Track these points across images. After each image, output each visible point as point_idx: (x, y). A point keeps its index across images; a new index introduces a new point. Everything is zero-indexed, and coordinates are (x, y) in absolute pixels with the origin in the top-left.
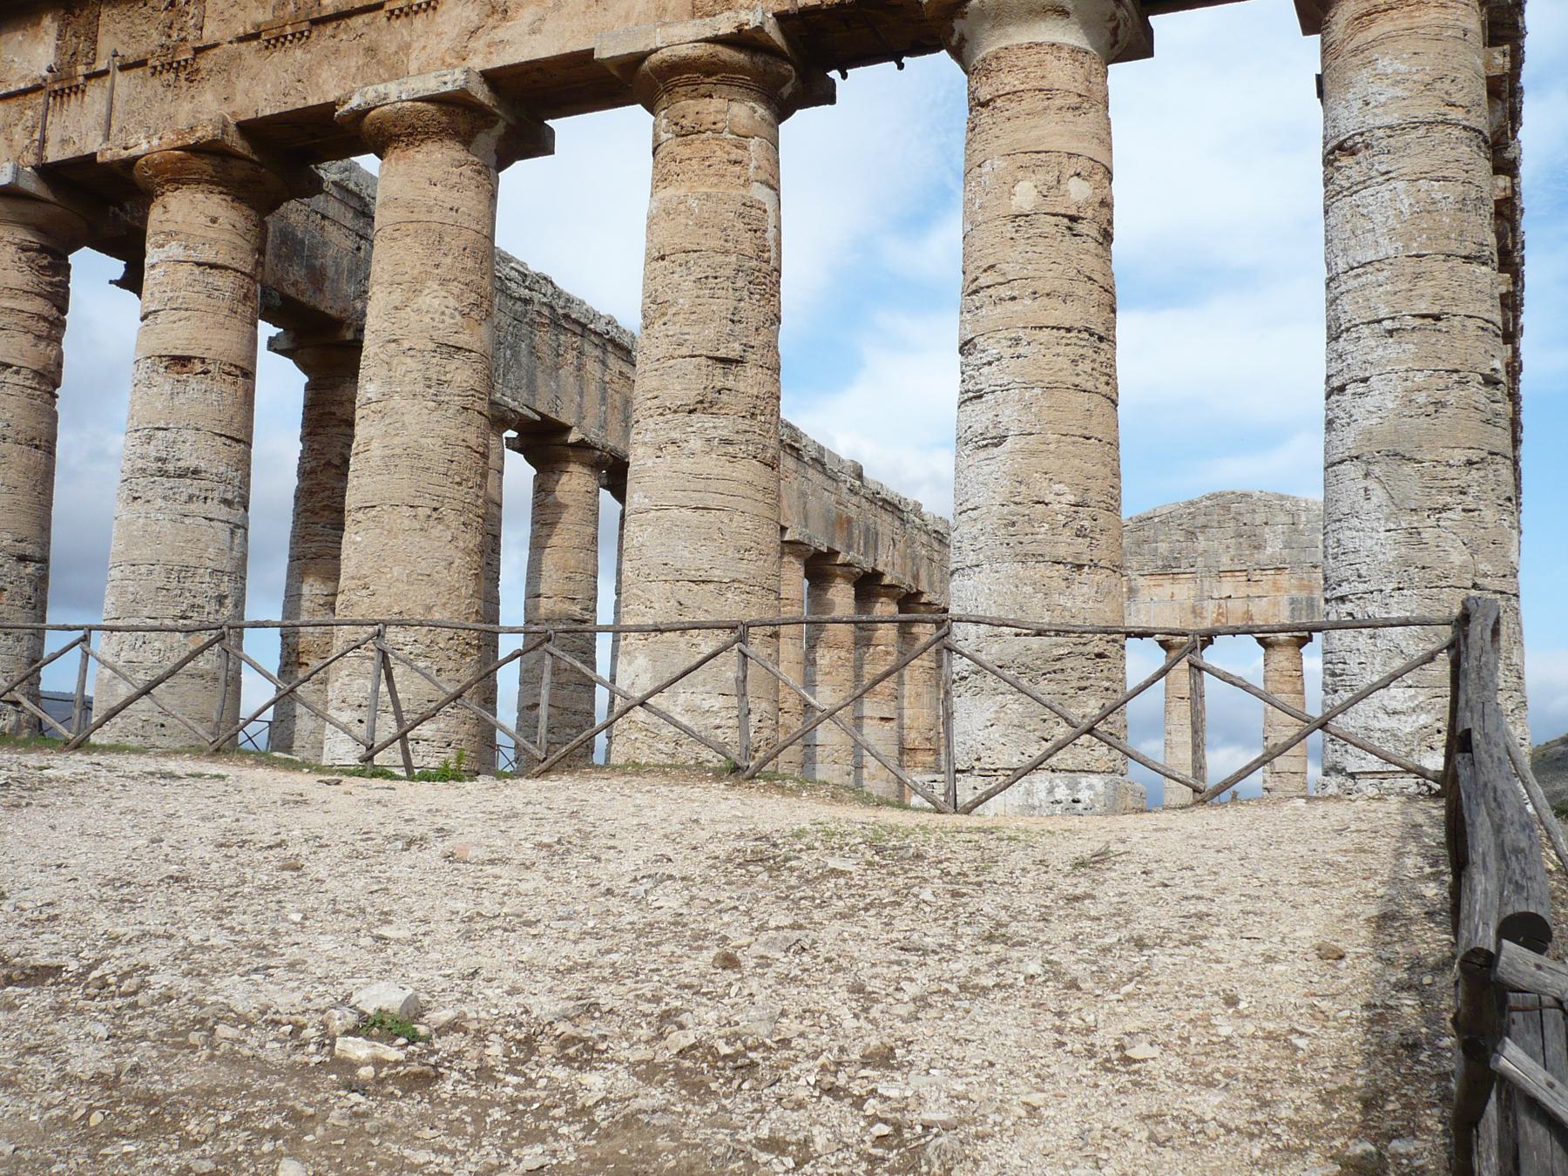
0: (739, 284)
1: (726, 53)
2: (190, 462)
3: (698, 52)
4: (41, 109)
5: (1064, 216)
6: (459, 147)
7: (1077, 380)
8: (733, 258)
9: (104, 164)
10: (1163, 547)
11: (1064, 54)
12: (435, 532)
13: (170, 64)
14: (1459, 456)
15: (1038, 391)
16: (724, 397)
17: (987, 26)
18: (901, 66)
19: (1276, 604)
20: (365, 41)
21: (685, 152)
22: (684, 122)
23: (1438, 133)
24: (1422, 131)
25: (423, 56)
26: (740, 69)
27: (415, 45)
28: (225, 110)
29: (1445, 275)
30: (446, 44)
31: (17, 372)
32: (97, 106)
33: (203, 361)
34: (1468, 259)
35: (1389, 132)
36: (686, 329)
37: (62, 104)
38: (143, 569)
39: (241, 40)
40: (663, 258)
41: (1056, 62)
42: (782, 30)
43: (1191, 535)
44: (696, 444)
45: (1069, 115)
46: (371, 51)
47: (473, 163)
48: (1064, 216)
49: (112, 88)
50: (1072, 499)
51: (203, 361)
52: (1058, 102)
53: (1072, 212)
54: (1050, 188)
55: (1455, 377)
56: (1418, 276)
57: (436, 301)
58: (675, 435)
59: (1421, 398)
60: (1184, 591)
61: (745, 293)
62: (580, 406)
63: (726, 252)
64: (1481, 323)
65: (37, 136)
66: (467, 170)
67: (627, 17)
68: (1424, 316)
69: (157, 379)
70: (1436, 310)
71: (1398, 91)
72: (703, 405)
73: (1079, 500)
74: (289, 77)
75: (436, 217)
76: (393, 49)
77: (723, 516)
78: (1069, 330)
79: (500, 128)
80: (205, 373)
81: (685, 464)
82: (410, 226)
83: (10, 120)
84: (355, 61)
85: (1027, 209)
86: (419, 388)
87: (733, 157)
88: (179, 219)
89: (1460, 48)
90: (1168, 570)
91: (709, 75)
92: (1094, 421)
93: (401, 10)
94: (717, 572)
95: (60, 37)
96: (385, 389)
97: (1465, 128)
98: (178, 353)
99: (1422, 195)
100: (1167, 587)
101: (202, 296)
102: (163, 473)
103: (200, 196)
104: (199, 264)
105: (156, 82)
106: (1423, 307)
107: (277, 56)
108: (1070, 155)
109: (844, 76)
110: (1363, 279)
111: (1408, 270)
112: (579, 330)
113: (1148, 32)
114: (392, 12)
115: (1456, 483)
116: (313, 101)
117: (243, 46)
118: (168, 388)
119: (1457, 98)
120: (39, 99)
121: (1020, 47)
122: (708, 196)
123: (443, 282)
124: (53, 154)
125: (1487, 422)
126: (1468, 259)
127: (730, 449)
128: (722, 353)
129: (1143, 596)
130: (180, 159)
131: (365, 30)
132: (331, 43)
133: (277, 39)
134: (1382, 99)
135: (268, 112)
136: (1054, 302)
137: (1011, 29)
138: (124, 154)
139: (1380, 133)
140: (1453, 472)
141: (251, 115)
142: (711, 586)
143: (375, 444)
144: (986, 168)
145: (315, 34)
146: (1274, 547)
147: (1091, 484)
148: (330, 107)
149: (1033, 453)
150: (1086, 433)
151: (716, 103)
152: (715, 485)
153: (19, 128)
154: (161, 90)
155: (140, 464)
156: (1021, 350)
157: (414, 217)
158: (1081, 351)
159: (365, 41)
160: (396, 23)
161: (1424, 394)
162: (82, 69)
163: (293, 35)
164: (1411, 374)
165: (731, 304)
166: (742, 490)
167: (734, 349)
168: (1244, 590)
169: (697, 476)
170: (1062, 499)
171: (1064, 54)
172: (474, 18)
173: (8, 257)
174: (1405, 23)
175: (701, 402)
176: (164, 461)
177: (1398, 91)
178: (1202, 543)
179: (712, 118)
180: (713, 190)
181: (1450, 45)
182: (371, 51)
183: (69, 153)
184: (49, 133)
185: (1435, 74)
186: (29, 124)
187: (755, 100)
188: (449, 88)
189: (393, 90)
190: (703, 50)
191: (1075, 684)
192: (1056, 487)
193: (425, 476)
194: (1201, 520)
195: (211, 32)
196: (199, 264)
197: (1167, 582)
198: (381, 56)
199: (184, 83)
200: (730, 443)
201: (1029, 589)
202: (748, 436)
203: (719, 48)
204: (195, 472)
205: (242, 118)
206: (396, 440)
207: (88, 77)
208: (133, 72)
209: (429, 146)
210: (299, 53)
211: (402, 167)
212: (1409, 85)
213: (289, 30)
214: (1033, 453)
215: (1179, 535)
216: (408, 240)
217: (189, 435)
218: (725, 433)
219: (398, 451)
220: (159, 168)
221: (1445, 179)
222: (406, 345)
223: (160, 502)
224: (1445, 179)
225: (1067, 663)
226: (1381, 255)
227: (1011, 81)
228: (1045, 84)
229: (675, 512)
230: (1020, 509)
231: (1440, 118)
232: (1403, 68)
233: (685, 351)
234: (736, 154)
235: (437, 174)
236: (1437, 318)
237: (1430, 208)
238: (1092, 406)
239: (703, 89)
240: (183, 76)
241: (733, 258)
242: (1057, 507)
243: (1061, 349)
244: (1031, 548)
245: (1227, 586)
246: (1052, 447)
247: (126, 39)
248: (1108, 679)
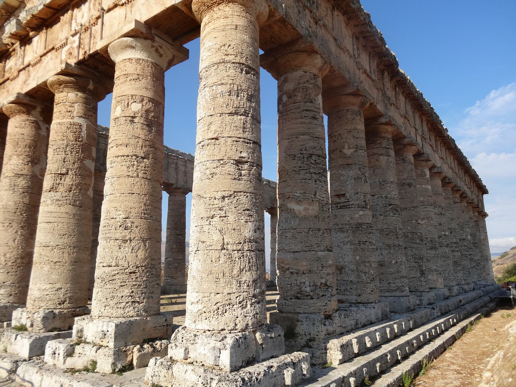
0: (68, 149)
1: (62, 78)
3: (55, 79)
5: (129, 117)
7: (129, 174)
8: (66, 141)
11: (134, 61)
12: (10, 230)
14: (219, 195)
15: (115, 179)
23: (221, 67)
24: (216, 66)
26: (69, 82)
29: (220, 122)
34: (231, 114)
35: (206, 69)
41: (130, 65)
42: (81, 69)
45: (133, 82)
47: (30, 120)
48: (129, 117)
50: (124, 216)
52: (128, 79)
53: (132, 115)
54: (125, 108)
55: (222, 162)
56: (211, 123)
59: (208, 172)
61: (69, 152)
62: (177, 178)
64: (236, 139)
66: (27, 123)
68: (213, 139)
70: (215, 136)
73: (126, 216)
75: (17, 137)
77: (56, 224)
78: (128, 156)
79: (39, 109)
85: (118, 116)
87: (68, 110)
89: (233, 32)
91: (60, 85)
92: (136, 187)
97: (234, 63)
99: (214, 91)
106: (211, 136)
108: (132, 96)
111: (208, 121)
112: (176, 158)
113: (188, 51)
115: (217, 206)
119: (230, 51)
123: (18, 155)
125: (235, 179)
126: (231, 114)
127: (60, 203)
128: (59, 172)
140: (216, 202)
142: (50, 248)
147: (132, 210)
150: (132, 192)
151: (64, 94)
152: (54, 215)
158: (132, 163)
161: (208, 170)
164: (205, 163)
165: (63, 156)
166: (63, 215)
167: (64, 171)
170: (121, 217)
171: (134, 61)
174: (212, 27)
175: (53, 188)
177: (209, 54)
179: (62, 99)
180: (62, 121)
181: (229, 31)
185: (221, 44)
187: (78, 91)
191: (119, 284)
192: (118, 213)
202: (67, 198)
203: (60, 76)
209: (17, 116)
212: (212, 50)
221: (222, 84)
224: (222, 84)
225: (117, 277)
228: (126, 73)
231: (222, 61)
234: (69, 109)
236: (217, 139)
238: (135, 182)
239: (61, 90)
242: (118, 220)
243: (124, 164)
246: (118, 198)
248: (135, 281)
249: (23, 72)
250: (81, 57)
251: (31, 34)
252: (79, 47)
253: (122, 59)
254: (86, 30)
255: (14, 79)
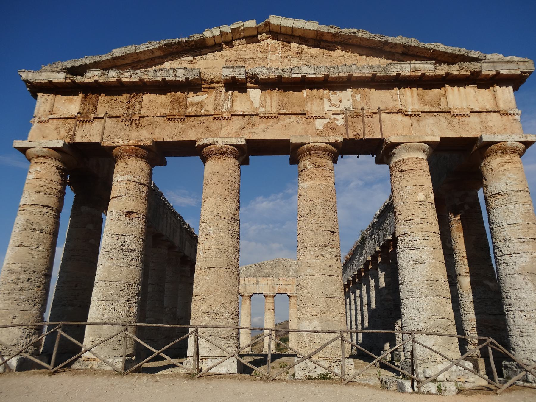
1: (330, 147)
2: (133, 247)
4: (73, 125)
6: (235, 160)
9: (103, 146)
10: (265, 271)
13: (130, 120)
16: (333, 242)
17: (404, 151)
18: (358, 157)
19: (293, 287)
20: (205, 125)
21: (318, 172)
22: (316, 164)
25: (226, 132)
27: (223, 129)
28: (151, 137)
30: (234, 130)
31: (52, 210)
32: (98, 128)
33: (137, 214)
36: (322, 222)
37: (83, 125)
38: (115, 283)
39: (157, 116)
40: (311, 201)
43: (272, 269)
44: (328, 256)
46: (207, 128)
49: (105, 123)
51: (137, 214)
56: (528, 228)
57: (231, 205)
58: (322, 253)
60: (270, 282)
63: (330, 202)
65: (71, 133)
67: (296, 132)
69: (121, 218)
71: (515, 182)
72: (328, 245)
74: (176, 131)
76: (215, 128)
80: (138, 218)
81: (326, 262)
82: (223, 181)
83: (59, 126)
84: (201, 130)
85: (422, 200)
86: (227, 231)
88: (132, 168)
90: (267, 277)
93: (219, 118)
94: (337, 295)
95: (83, 103)
96: (217, 231)
98: (130, 210)
100: (266, 282)
101: (138, 193)
102: (123, 250)
103: (139, 161)
104: (137, 183)
105: (123, 124)
106: (532, 236)
107: (172, 124)
109: (342, 157)
110: (513, 228)
114: (215, 118)
116: (186, 139)
117: (158, 118)
118: (126, 222)
120: (73, 122)
121: (415, 158)
122: (325, 185)
124: (78, 140)
127: (336, 258)
129: (260, 283)
130: (136, 150)
131: (205, 121)
132: (192, 123)
133: (172, 119)
134: (511, 184)
135: (168, 140)
136: (432, 226)
137: (411, 153)
138: (113, 145)
139: (512, 192)
141: (161, 140)
142: (336, 299)
143: (213, 247)
144: (408, 188)
145: (186, 120)
146: (292, 273)
148: (194, 142)
149: (434, 266)
153: (63, 129)
154: (125, 127)
155: (114, 246)
156: (427, 238)
157: (224, 178)
159: (205, 125)
160: (216, 121)
162: (93, 115)
163: (179, 119)
168: (285, 283)
169: (330, 266)
172: (243, 124)
173: (53, 170)
174: (514, 166)
176: (123, 246)
177: (515, 182)
178: (275, 271)
179: (324, 164)
182: (207, 128)
183: (85, 140)
184: (76, 133)
186: (68, 129)
188: (240, 143)
189: (220, 141)
190: (325, 145)
192: (441, 276)
193: (230, 259)
194: (275, 265)
195: (144, 112)
196: (137, 183)
197: (266, 279)
198: (211, 130)
199: (135, 127)
200: (335, 256)
201: (439, 305)
203: (329, 145)
204: (134, 250)
205: (158, 140)
206: (221, 247)
207: (94, 118)
208: (113, 119)
209: (227, 158)
210: (180, 124)
211: (220, 163)
213: (177, 117)
214: (434, 266)
215: (270, 269)
216: (222, 185)
217: (132, 238)
218: (335, 253)
219: (222, 250)
220: (125, 151)
222: (223, 217)
223: (122, 260)
226: (518, 222)
227: (413, 167)
228: (421, 168)
229: (324, 276)
230: (433, 282)
232: (515, 177)
233: (322, 228)
235: (231, 167)
236: (534, 239)
237: (527, 212)
239: (321, 156)
240: (134, 123)
241: (332, 203)
244: (438, 293)
245: (281, 282)
247: (109, 109)
249: (240, 117)
250: (351, 136)
251: (249, 85)
252: (346, 126)
253: (416, 156)
254: (358, 116)
255: (222, 119)
